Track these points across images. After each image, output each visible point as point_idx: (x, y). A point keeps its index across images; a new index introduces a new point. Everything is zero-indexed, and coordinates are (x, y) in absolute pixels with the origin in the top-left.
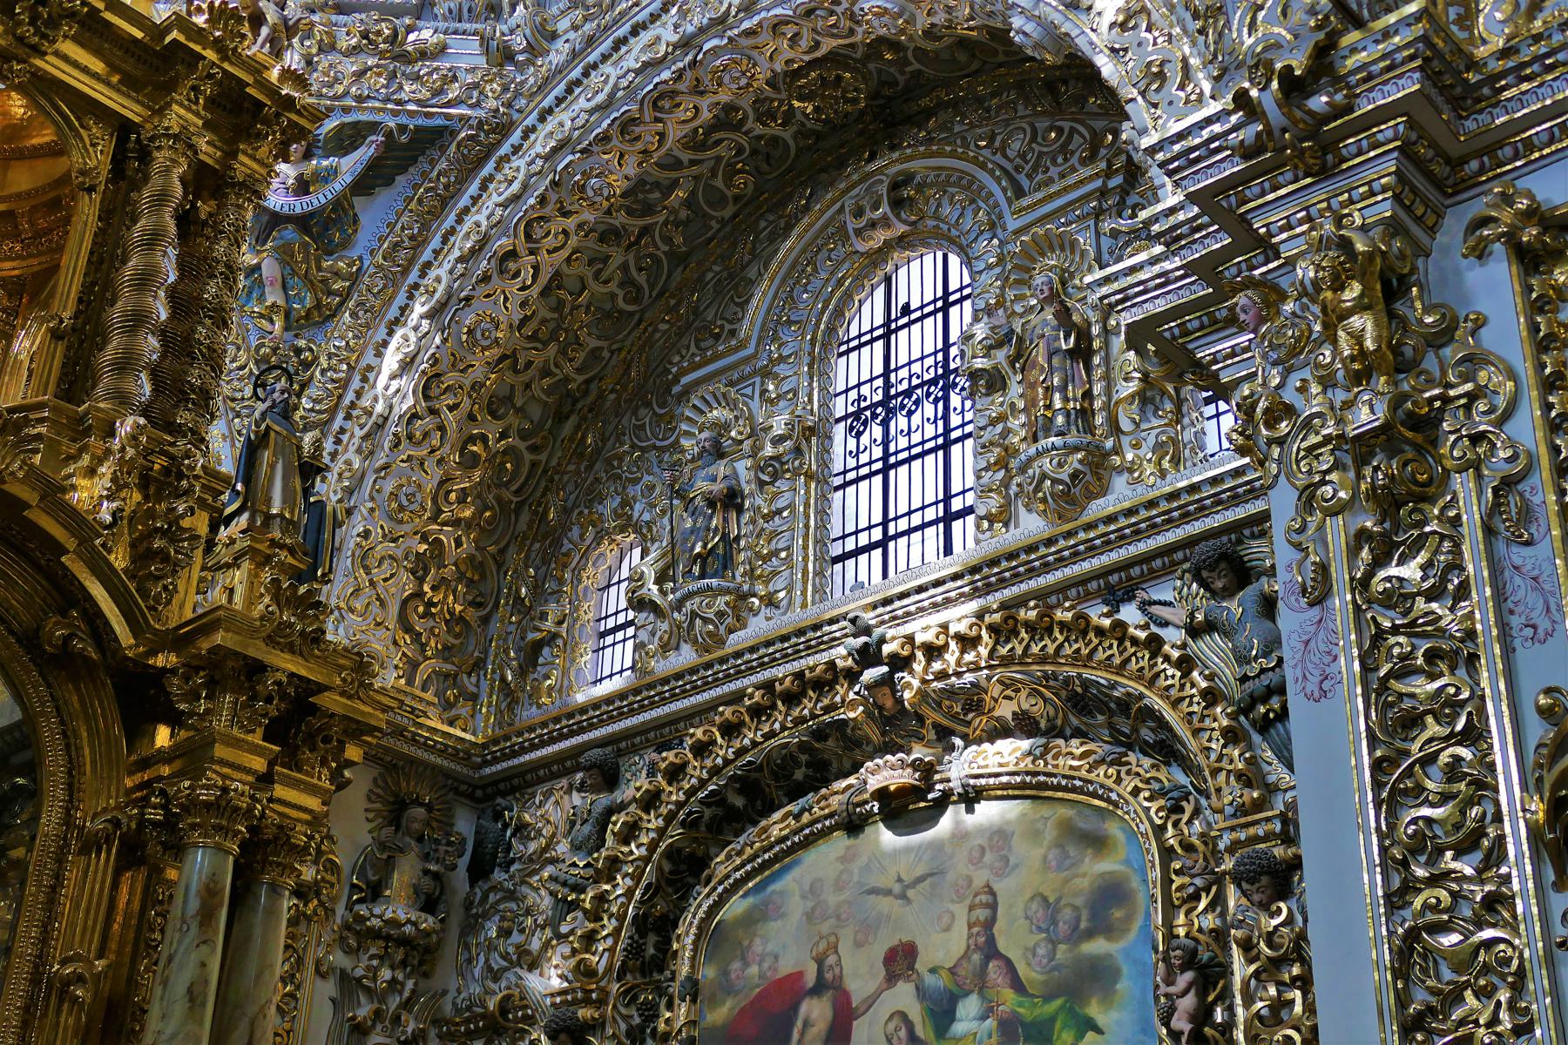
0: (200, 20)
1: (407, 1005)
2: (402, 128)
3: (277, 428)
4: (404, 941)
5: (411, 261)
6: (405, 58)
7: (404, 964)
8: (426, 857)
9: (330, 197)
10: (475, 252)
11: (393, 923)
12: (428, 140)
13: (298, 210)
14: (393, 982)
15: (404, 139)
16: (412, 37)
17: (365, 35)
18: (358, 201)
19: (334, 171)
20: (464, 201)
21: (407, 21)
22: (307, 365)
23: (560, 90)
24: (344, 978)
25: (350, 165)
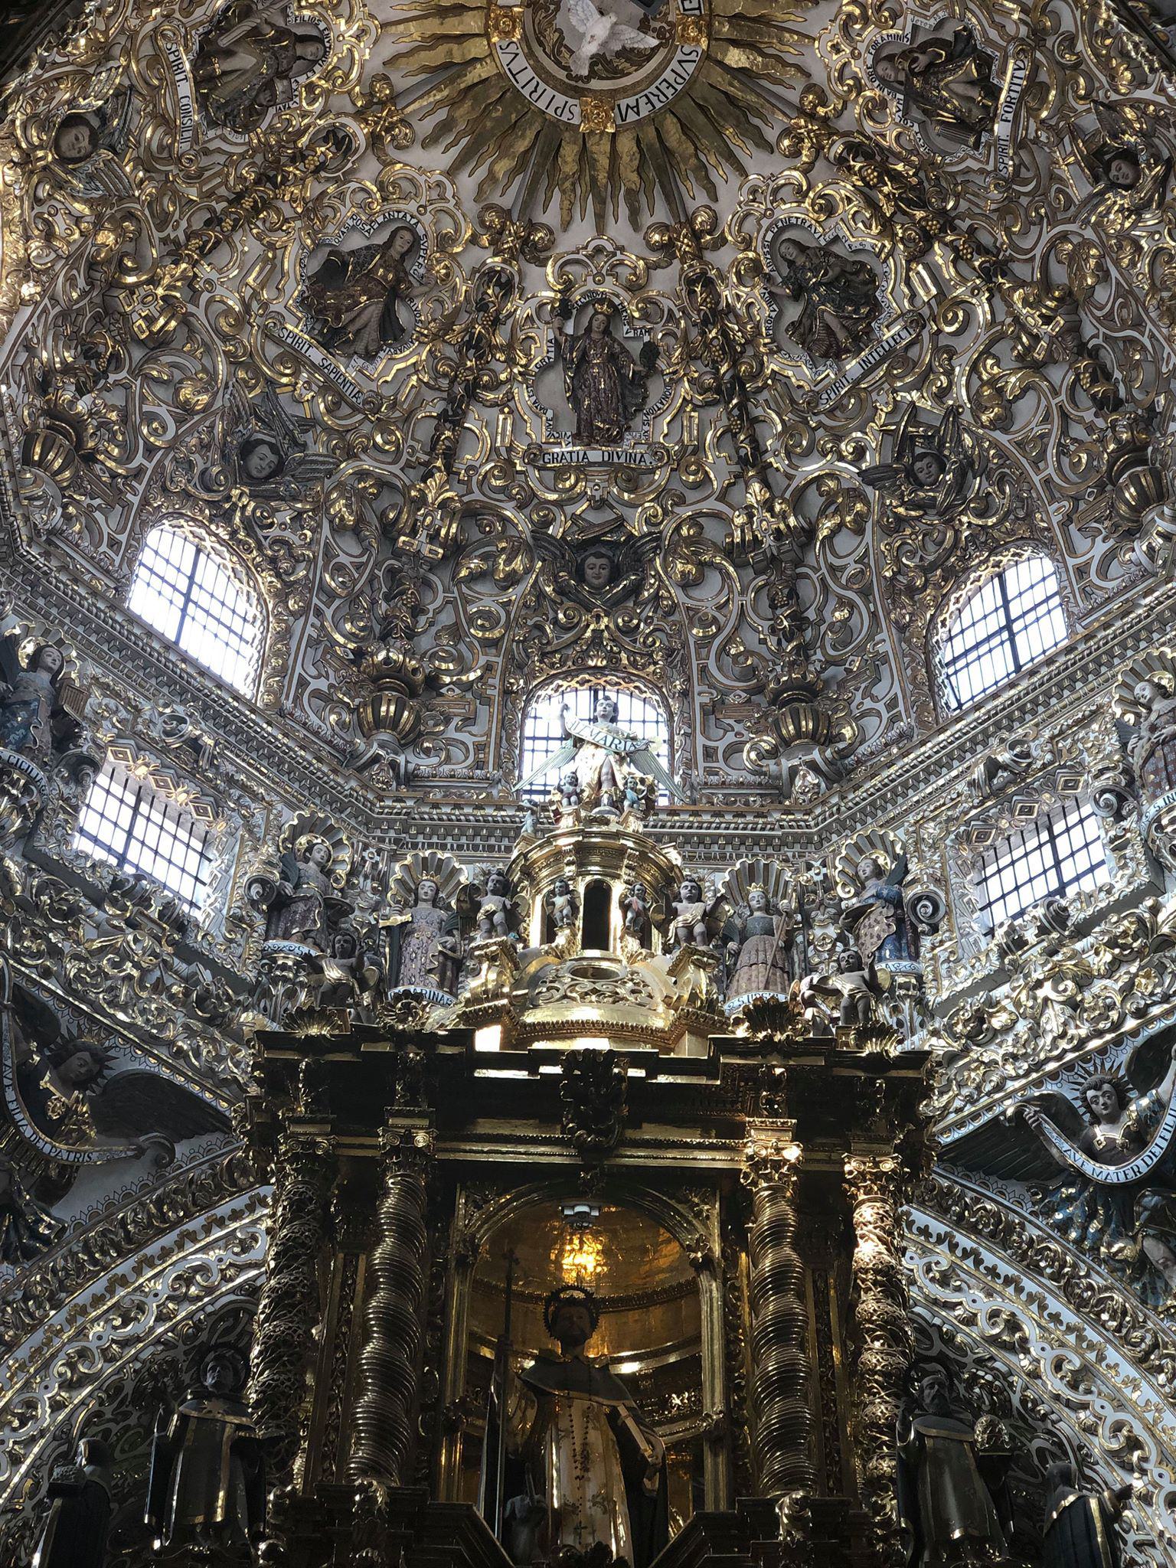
0: (741, 1032)
3: (933, 1432)
9: (1168, 1136)
13: (1144, 1170)
16: (1161, 918)
17: (1112, 944)
21: (1149, 902)
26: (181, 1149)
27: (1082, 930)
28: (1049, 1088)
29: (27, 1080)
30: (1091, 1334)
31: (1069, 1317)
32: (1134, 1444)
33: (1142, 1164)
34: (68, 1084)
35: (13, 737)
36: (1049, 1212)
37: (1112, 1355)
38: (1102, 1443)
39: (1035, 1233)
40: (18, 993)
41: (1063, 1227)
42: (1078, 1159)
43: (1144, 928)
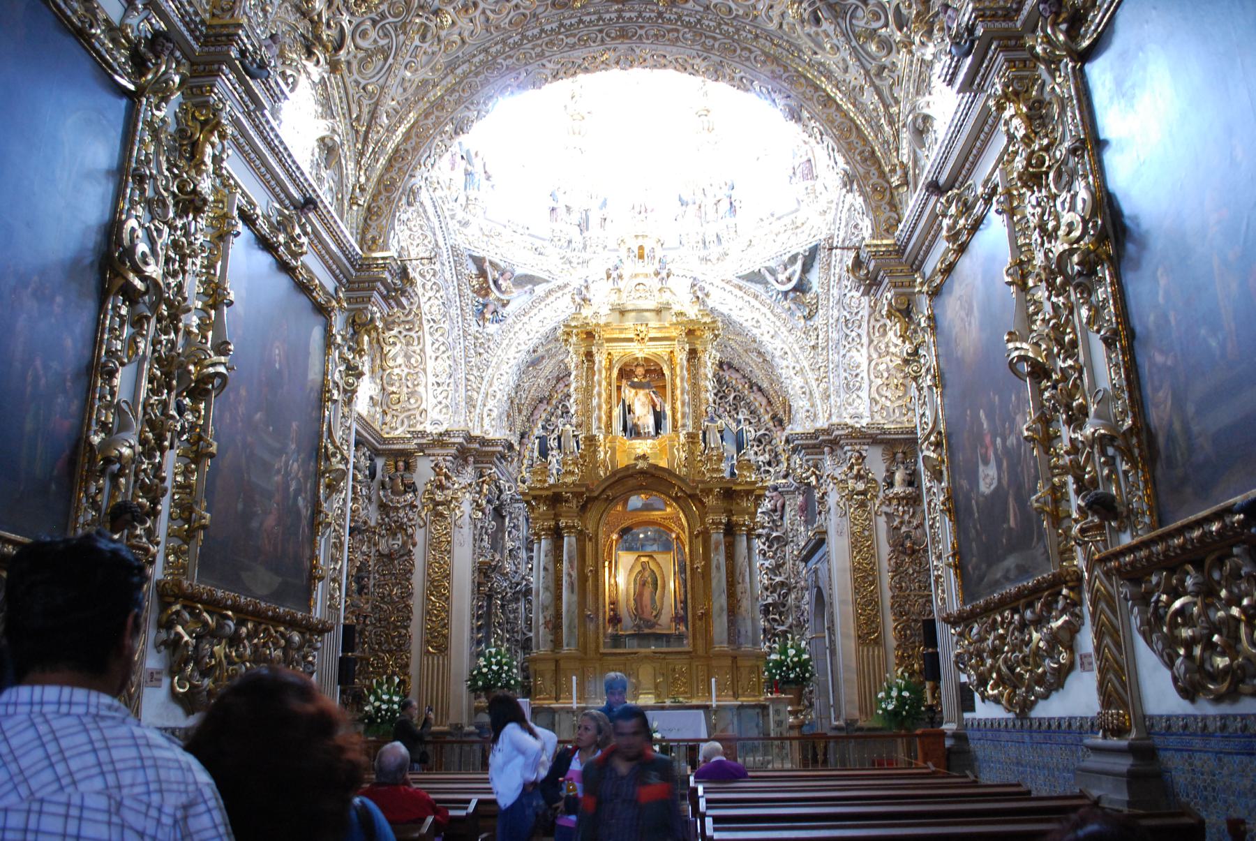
1: (913, 516)
2: (805, 251)
4: (903, 498)
5: (829, 286)
6: (797, 227)
7: (907, 504)
8: (906, 469)
10: (840, 279)
11: (897, 494)
12: (814, 252)
14: (904, 512)
15: (807, 254)
18: (807, 275)
19: (794, 272)
20: (833, 263)
22: (816, 329)
23: (838, 221)
24: (886, 514)
25: (798, 266)
26: (536, 288)
27: (779, 219)
28: (767, 264)
29: (495, 282)
30: (778, 324)
31: (773, 318)
32: (786, 353)
33: (790, 286)
34: (505, 280)
35: (476, 186)
36: (767, 292)
37: (783, 329)
38: (778, 353)
39: (763, 297)
40: (491, 263)
41: (771, 296)
42: (775, 283)
43: (793, 222)
